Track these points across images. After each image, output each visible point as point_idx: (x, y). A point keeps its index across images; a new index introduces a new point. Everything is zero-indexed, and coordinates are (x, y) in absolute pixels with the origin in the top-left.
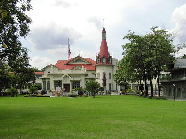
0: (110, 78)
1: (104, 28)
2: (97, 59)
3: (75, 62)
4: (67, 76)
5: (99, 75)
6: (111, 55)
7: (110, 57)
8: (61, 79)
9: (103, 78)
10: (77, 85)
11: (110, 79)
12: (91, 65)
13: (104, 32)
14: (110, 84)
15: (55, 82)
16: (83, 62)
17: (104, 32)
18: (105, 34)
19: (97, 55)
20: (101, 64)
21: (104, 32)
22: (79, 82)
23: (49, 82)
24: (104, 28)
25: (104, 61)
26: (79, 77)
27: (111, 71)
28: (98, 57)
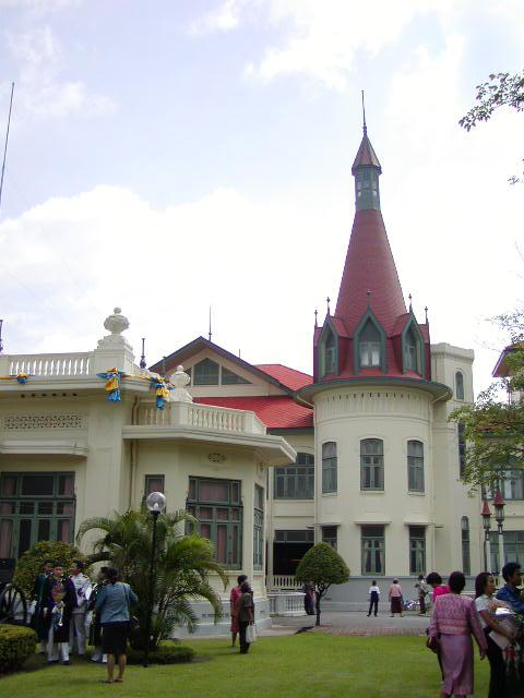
0: (416, 482)
1: (366, 148)
2: (323, 346)
5: (334, 459)
6: (421, 321)
7: (417, 333)
11: (422, 489)
12: (288, 396)
13: (366, 168)
14: (417, 532)
16: (231, 379)
17: (366, 168)
19: (320, 325)
20: (346, 374)
21: (365, 162)
22: (66, 479)
24: (366, 148)
25: (372, 358)
26: (73, 421)
27: (420, 432)
28: (325, 337)
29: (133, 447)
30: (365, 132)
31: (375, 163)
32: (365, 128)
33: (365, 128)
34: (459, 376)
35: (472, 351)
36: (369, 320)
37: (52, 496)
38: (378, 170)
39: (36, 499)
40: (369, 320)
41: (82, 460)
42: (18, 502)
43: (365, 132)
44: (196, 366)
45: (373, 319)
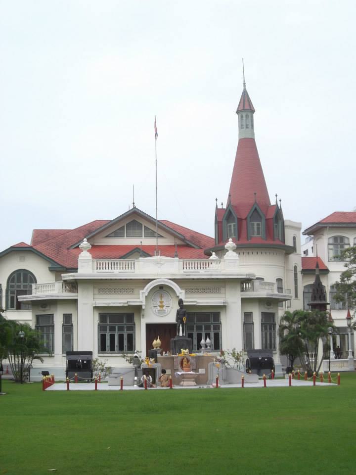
3: (118, 234)
4: (161, 287)
8: (139, 298)
9: (314, 298)
10: (208, 328)
13: (246, 109)
15: (103, 318)
16: (152, 234)
17: (246, 109)
18: (252, 117)
22: (217, 316)
23: (68, 318)
29: (244, 301)
30: (245, 86)
32: (244, 84)
33: (244, 84)
34: (294, 238)
35: (300, 223)
36: (256, 209)
37: (210, 323)
39: (203, 324)
40: (256, 209)
41: (224, 307)
42: (195, 325)
43: (245, 86)
44: (127, 224)
45: (258, 208)
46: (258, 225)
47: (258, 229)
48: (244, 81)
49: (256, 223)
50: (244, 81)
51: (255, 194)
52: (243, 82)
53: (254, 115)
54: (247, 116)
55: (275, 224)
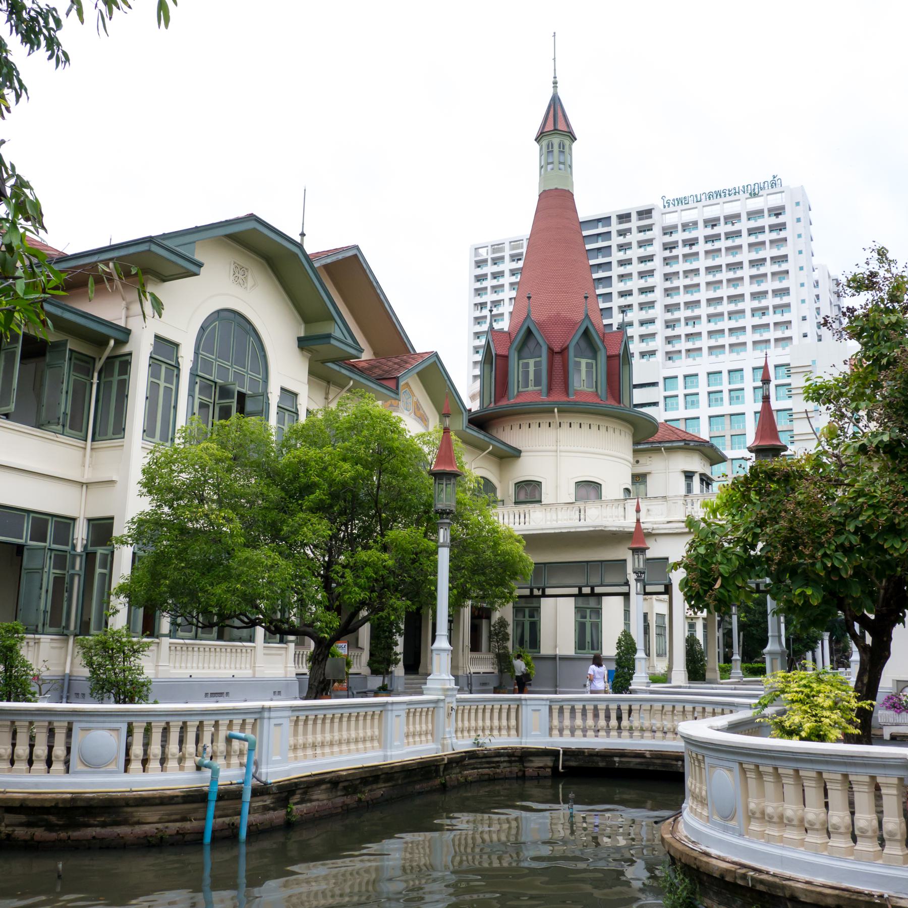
1: (555, 105)
13: (556, 131)
17: (556, 131)
24: (555, 105)
31: (561, 126)
32: (555, 83)
33: (555, 83)
36: (529, 332)
38: (573, 138)
40: (529, 332)
46: (537, 364)
47: (537, 374)
48: (555, 77)
49: (531, 362)
50: (555, 77)
51: (529, 298)
52: (553, 79)
53: (575, 145)
54: (550, 146)
55: (584, 362)
